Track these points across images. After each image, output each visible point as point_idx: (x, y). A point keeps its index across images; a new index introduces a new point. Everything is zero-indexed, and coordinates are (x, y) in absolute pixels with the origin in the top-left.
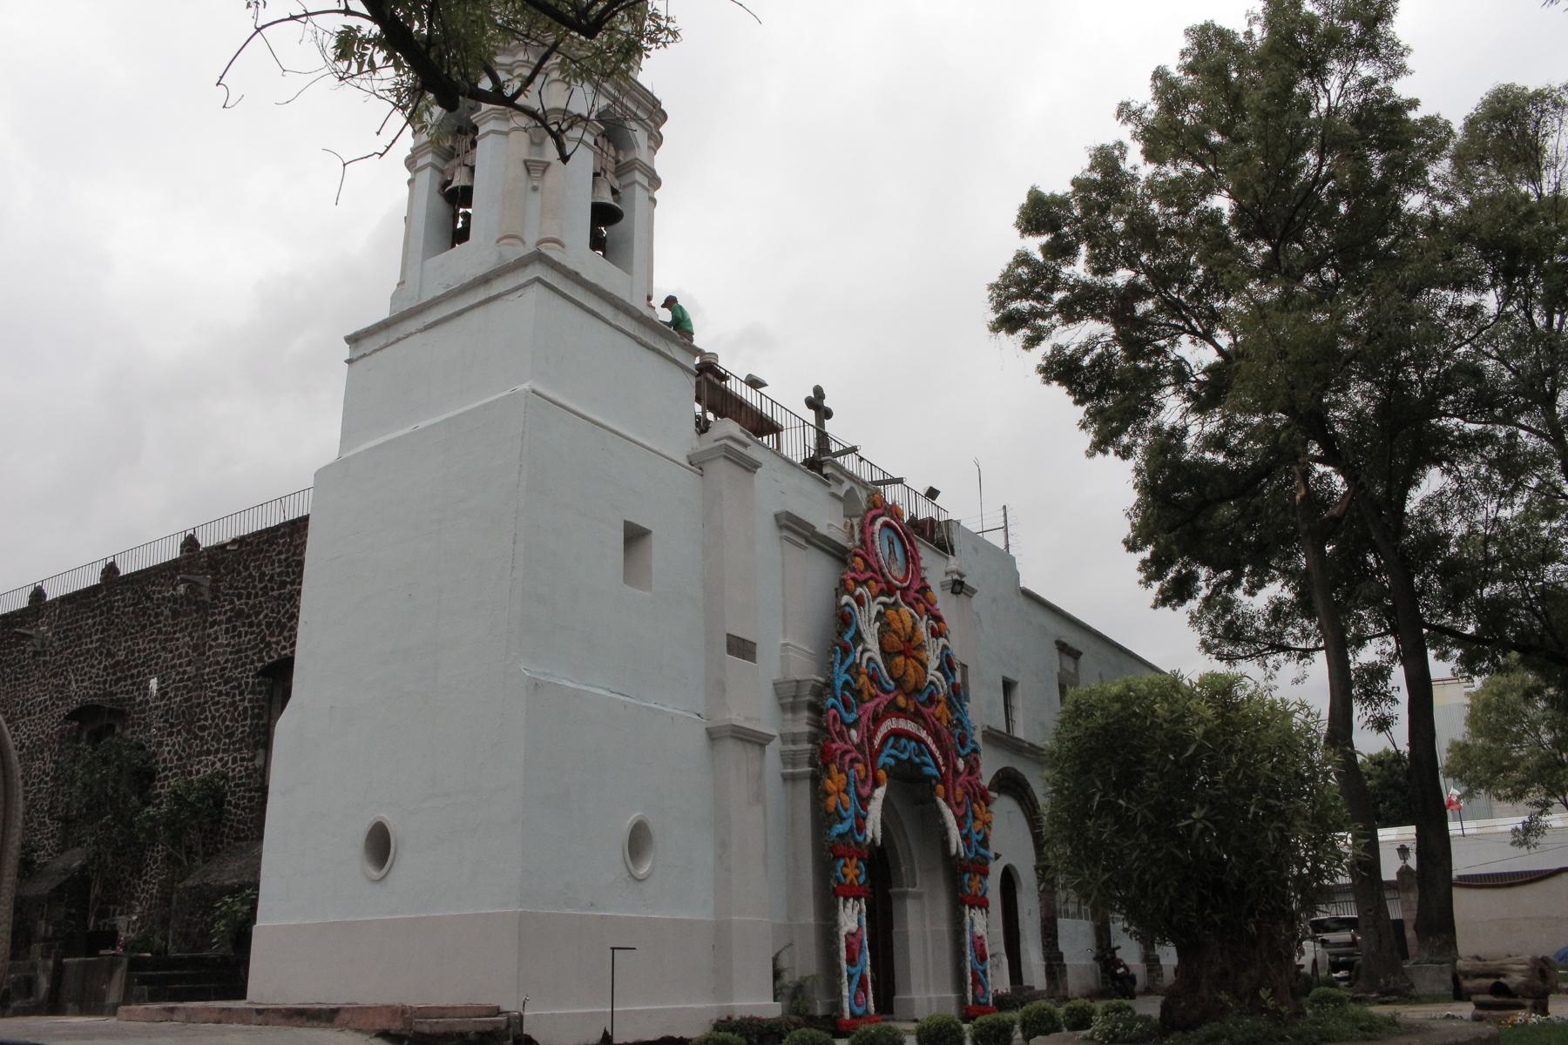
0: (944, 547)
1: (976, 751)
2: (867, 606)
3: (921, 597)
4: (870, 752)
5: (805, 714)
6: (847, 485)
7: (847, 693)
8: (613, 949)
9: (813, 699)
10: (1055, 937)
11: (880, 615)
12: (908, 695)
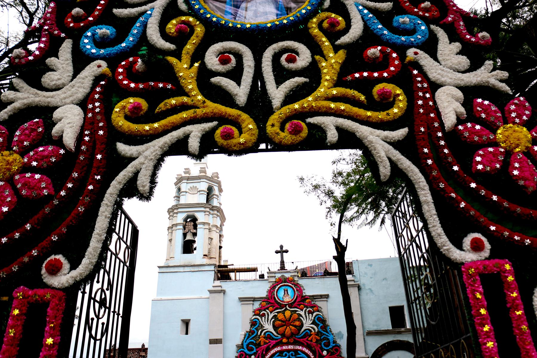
6: (278, 276)
11: (275, 316)
12: (288, 338)
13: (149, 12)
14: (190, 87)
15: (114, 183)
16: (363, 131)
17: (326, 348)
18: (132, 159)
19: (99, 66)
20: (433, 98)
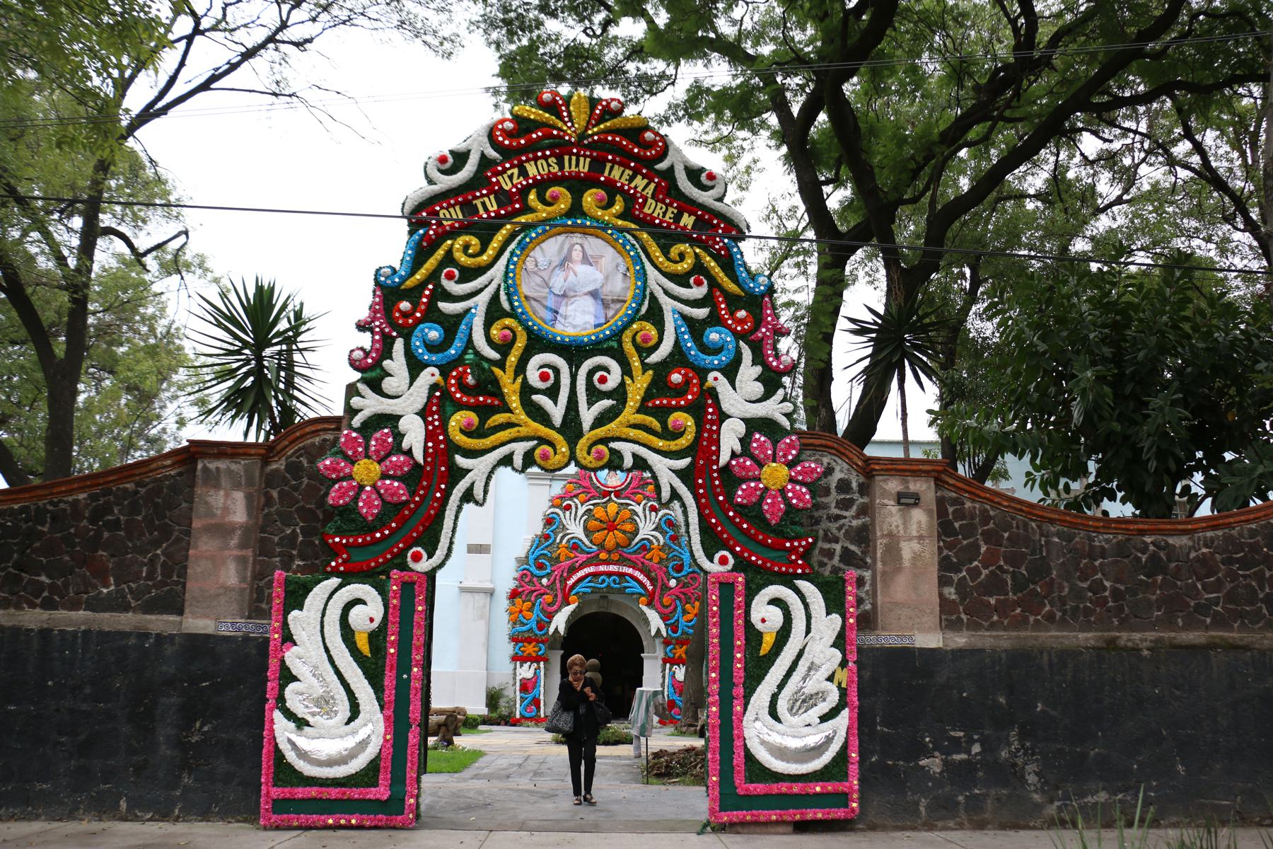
4: (564, 589)
12: (609, 552)
13: (473, 311)
14: (514, 405)
15: (455, 491)
16: (653, 459)
17: (675, 575)
18: (469, 471)
19: (433, 375)
20: (718, 432)
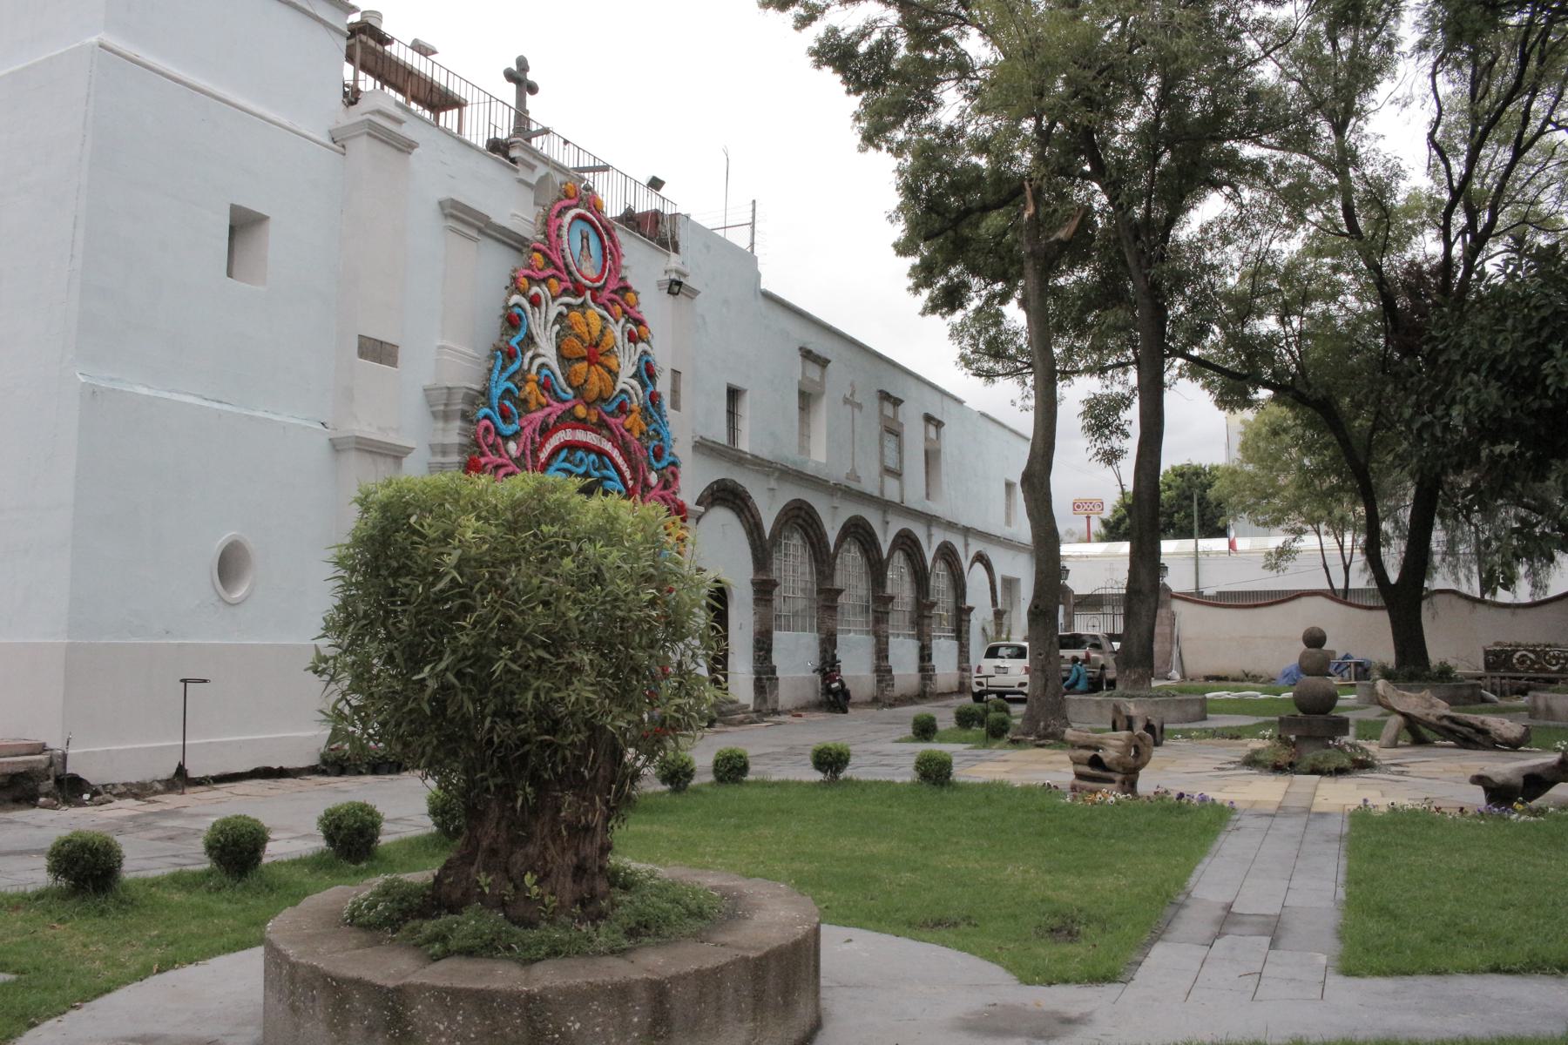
0: (669, 244)
1: (674, 464)
2: (543, 308)
3: (617, 298)
5: (457, 424)
6: (541, 170)
7: (507, 403)
8: (185, 681)
9: (467, 408)
10: (769, 651)
11: (560, 314)
12: (589, 405)
